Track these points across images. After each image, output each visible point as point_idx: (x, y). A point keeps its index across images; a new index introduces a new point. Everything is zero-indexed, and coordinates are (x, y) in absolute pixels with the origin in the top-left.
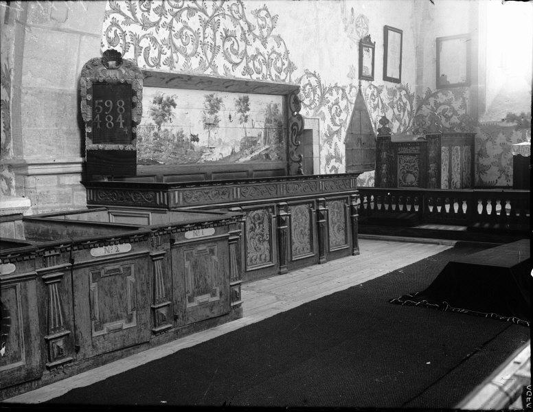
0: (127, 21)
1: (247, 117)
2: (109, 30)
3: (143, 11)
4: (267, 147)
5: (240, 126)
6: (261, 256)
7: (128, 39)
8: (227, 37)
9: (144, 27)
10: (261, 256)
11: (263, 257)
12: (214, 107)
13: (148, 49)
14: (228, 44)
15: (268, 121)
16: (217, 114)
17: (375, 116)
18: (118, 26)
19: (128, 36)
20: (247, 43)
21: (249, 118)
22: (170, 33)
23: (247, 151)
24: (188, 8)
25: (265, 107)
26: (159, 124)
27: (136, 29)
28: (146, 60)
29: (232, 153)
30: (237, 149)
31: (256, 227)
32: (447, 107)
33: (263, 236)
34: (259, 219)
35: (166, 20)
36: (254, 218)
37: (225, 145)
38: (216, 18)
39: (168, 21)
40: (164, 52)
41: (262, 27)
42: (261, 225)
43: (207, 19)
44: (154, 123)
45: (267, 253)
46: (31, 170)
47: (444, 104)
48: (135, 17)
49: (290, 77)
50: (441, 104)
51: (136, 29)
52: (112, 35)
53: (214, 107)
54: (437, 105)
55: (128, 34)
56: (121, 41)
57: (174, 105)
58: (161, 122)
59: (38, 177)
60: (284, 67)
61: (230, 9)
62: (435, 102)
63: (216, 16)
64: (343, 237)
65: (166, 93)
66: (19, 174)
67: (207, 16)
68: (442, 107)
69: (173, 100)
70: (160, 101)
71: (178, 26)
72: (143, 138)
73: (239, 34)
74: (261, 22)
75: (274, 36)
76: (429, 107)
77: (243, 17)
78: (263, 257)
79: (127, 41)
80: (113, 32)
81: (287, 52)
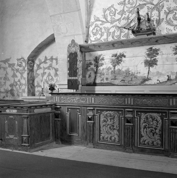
2: (94, 29)
3: (112, 16)
6: (111, 137)
7: (103, 30)
9: (111, 23)
10: (111, 137)
11: (113, 138)
12: (153, 53)
13: (114, 32)
14: (171, 16)
16: (156, 58)
19: (103, 29)
26: (114, 66)
27: (108, 25)
28: (113, 37)
29: (168, 80)
33: (113, 126)
34: (111, 116)
35: (125, 16)
36: (106, 115)
37: (164, 75)
38: (160, 4)
39: (126, 16)
40: (124, 31)
42: (112, 120)
43: (153, 6)
44: (111, 66)
45: (116, 137)
48: (106, 20)
51: (108, 25)
52: (94, 31)
53: (153, 53)
55: (103, 28)
56: (100, 32)
57: (125, 56)
58: (116, 65)
59: (63, 89)
63: (161, 2)
65: (119, 51)
67: (153, 5)
69: (123, 54)
70: (116, 55)
72: (105, 74)
78: (113, 138)
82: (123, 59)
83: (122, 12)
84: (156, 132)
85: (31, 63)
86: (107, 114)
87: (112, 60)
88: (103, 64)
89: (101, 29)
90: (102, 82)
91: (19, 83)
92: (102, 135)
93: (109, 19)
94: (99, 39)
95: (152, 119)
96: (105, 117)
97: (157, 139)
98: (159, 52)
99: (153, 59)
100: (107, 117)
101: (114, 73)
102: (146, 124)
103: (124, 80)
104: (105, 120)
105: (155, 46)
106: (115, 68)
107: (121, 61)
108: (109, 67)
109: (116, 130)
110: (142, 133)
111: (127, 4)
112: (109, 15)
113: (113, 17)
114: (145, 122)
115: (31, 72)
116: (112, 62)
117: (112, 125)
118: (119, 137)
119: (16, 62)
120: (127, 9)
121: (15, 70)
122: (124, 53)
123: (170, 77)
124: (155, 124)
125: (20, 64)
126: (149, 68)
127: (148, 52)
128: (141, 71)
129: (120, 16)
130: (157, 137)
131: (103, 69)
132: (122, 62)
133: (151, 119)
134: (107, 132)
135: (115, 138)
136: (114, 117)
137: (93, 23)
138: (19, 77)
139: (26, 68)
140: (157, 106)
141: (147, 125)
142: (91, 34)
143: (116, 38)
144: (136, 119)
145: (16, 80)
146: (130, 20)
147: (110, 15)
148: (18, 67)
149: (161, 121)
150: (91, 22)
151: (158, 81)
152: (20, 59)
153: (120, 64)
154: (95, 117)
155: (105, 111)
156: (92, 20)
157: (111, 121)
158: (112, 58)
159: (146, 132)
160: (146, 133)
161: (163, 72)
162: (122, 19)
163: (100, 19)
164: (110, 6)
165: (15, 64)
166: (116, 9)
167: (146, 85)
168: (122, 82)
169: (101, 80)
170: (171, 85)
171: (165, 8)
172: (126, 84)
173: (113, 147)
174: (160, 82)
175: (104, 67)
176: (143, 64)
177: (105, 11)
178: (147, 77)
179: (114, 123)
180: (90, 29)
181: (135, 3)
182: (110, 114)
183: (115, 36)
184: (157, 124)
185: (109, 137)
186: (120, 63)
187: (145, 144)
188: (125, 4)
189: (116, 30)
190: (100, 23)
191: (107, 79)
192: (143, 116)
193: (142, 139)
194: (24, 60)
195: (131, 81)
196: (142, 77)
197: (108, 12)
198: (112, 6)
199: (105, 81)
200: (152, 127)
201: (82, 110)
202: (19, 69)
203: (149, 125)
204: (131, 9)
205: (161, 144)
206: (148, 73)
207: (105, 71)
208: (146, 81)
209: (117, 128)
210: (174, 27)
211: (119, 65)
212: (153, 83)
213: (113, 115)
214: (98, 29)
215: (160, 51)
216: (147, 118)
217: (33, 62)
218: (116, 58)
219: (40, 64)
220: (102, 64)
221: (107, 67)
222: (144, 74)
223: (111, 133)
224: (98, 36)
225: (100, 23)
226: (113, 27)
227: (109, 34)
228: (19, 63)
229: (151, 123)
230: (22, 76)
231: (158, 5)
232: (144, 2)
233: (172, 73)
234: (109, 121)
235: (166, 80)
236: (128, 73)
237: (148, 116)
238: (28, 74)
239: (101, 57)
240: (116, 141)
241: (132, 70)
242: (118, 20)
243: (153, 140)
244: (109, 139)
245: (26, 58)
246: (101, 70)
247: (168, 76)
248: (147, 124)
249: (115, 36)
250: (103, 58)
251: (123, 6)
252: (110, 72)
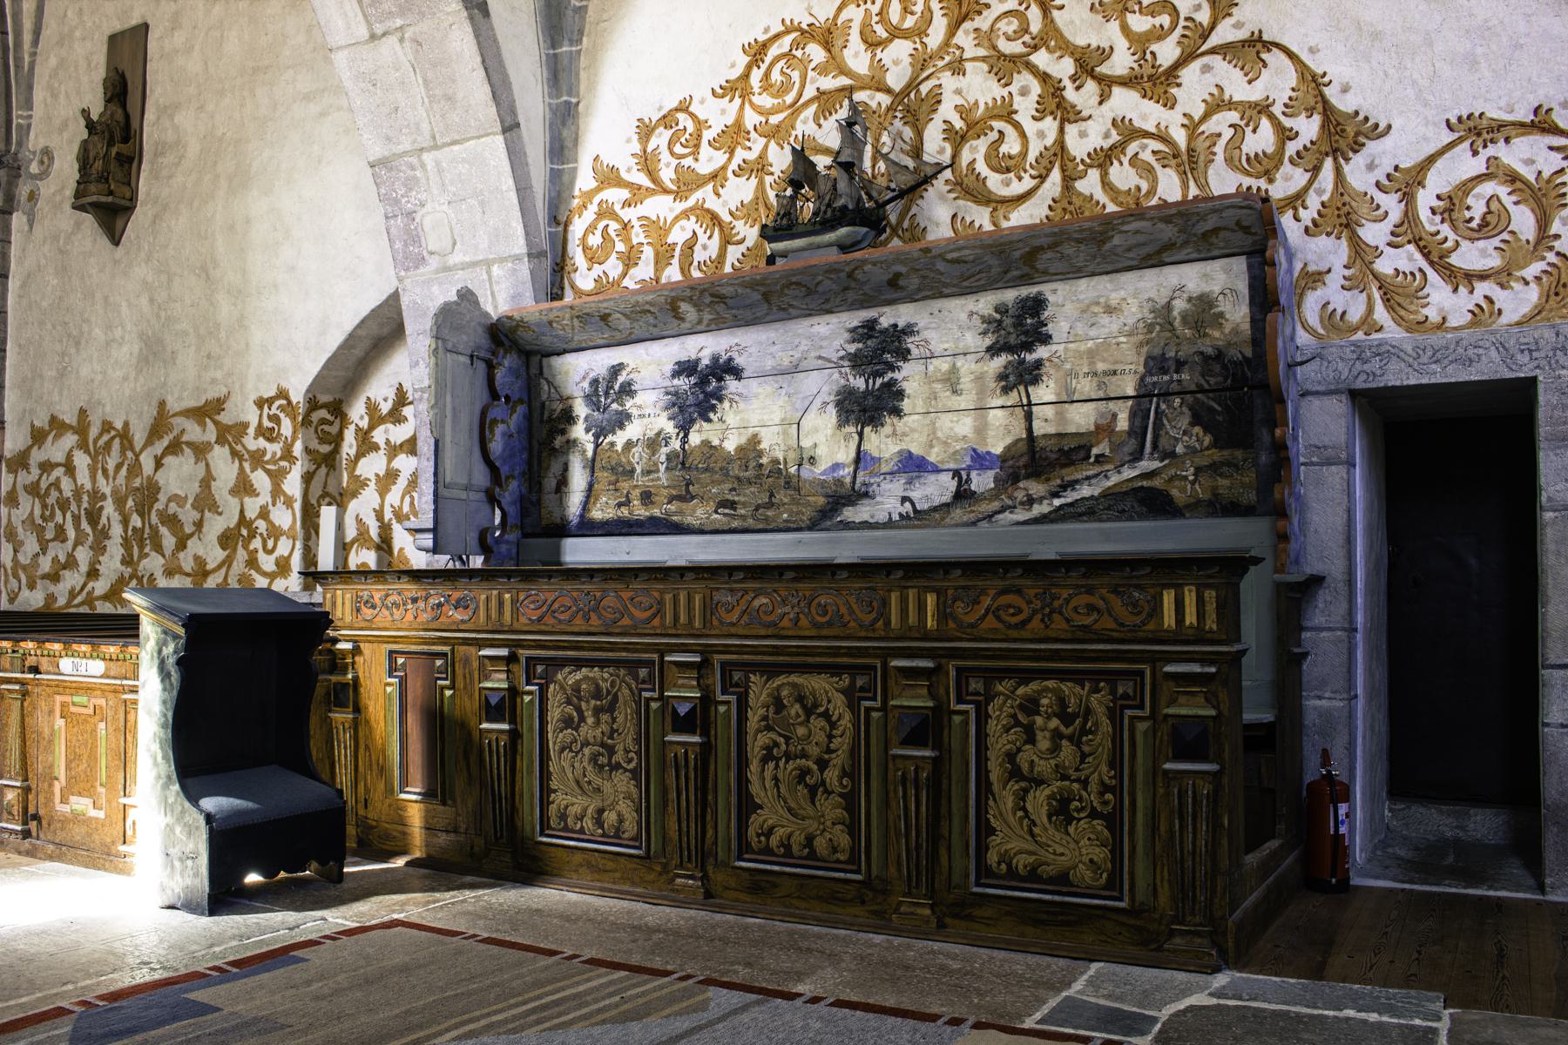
0: (637, 195)
1: (1039, 364)
2: (591, 229)
3: (683, 156)
4: (1147, 465)
5: (999, 402)
6: (601, 811)
7: (638, 236)
8: (972, 126)
9: (679, 195)
10: (601, 811)
11: (610, 817)
13: (690, 246)
14: (975, 153)
15: (1156, 364)
16: (896, 375)
18: (614, 216)
20: (1067, 114)
21: (1047, 368)
22: (761, 183)
23: (1036, 488)
24: (821, 93)
25: (1134, 312)
26: (685, 428)
27: (660, 207)
30: (982, 482)
31: (582, 719)
33: (611, 751)
36: (576, 689)
39: (752, 156)
40: (739, 238)
41: (1140, 43)
42: (605, 717)
43: (885, 100)
44: (670, 428)
45: (625, 807)
48: (654, 181)
49: (1338, 171)
52: (595, 240)
56: (620, 247)
57: (737, 373)
58: (692, 421)
60: (1292, 148)
61: (986, 38)
63: (927, 78)
64: (1100, 854)
65: (704, 347)
67: (888, 91)
69: (731, 359)
72: (639, 470)
73: (1025, 108)
74: (1139, 23)
75: (1223, 50)
77: (1049, 36)
79: (635, 241)
80: (598, 233)
81: (1313, 82)
82: (732, 385)
83: (733, 136)
84: (823, 783)
85: (323, 421)
86: (578, 682)
87: (676, 394)
88: (628, 417)
89: (626, 226)
90: (625, 512)
91: (261, 525)
92: (559, 800)
93: (667, 175)
94: (617, 283)
95: (804, 707)
96: (569, 702)
97: (829, 823)
98: (910, 343)
99: (879, 381)
100: (580, 699)
101: (683, 464)
102: (773, 735)
103: (732, 505)
104: (571, 718)
105: (886, 309)
106: (686, 436)
107: (720, 400)
108: (658, 434)
109: (626, 770)
110: (755, 788)
111: (756, 90)
112: (665, 156)
113: (688, 162)
114: (769, 728)
115: (323, 470)
116: (674, 405)
117: (603, 745)
118: (639, 811)
119: (252, 416)
120: (758, 119)
121: (246, 456)
122: (735, 355)
123: (969, 480)
124: (821, 737)
125: (270, 425)
126: (861, 435)
127: (852, 348)
128: (821, 451)
129: (720, 158)
130: (831, 808)
131: (629, 445)
132: (726, 404)
133: (797, 706)
134: (578, 782)
135: (619, 814)
136: (615, 698)
137: (589, 195)
138: (265, 498)
139: (298, 449)
140: (825, 632)
141: (776, 744)
142: (578, 257)
143: (696, 274)
144: (722, 709)
145: (252, 507)
146: (772, 174)
147: (672, 153)
148: (262, 442)
149: (848, 716)
150: (577, 193)
151: (907, 505)
152: (270, 401)
153: (711, 415)
154: (519, 700)
155: (567, 670)
156: (585, 180)
157: (598, 723)
158: (676, 382)
159: (776, 779)
160: (777, 785)
161: (932, 458)
162: (730, 174)
163: (624, 175)
164: (675, 104)
165: (246, 425)
166: (702, 117)
167: (848, 526)
168: (724, 515)
169: (620, 505)
170: (974, 524)
171: (947, 111)
172: (746, 525)
173: (610, 865)
174: (915, 510)
175: (633, 431)
176: (832, 412)
177: (646, 131)
178: (848, 480)
179: (613, 731)
180: (571, 228)
181: (797, 86)
182: (594, 681)
183: (695, 263)
184: (830, 737)
185: (590, 811)
186: (713, 408)
187: (768, 850)
188: (746, 94)
189: (700, 232)
190: (615, 195)
191: (647, 498)
192: (760, 691)
193: (755, 822)
194: (289, 403)
195: (770, 505)
196: (823, 484)
197: (660, 139)
198: (683, 107)
199: (641, 512)
200: (804, 755)
201: (457, 659)
202: (264, 452)
203: (787, 739)
204: (775, 120)
205: (852, 849)
206: (858, 460)
207: (638, 457)
208: (844, 505)
209: (630, 761)
210: (995, 210)
211: (709, 420)
212: (882, 517)
213: (608, 692)
214: (614, 226)
215: (917, 339)
216: (779, 705)
217: (338, 410)
218: (693, 380)
219: (372, 427)
220: (622, 420)
221: (651, 434)
222: (836, 466)
223: (598, 790)
224: (613, 267)
225: (624, 194)
226: (685, 214)
227: (662, 260)
228: (267, 423)
229: (801, 731)
230: (277, 491)
231: (912, 95)
232: (844, 81)
233: (980, 460)
234: (590, 720)
235: (947, 498)
236: (752, 464)
237: (785, 693)
238: (308, 478)
239: (621, 379)
240: (626, 835)
241: (773, 444)
242: (714, 176)
243: (812, 826)
244: (588, 823)
245: (298, 396)
246: (619, 448)
247: (956, 473)
248: (780, 735)
249: (695, 263)
250: (629, 384)
251: (738, 101)
252: (663, 458)
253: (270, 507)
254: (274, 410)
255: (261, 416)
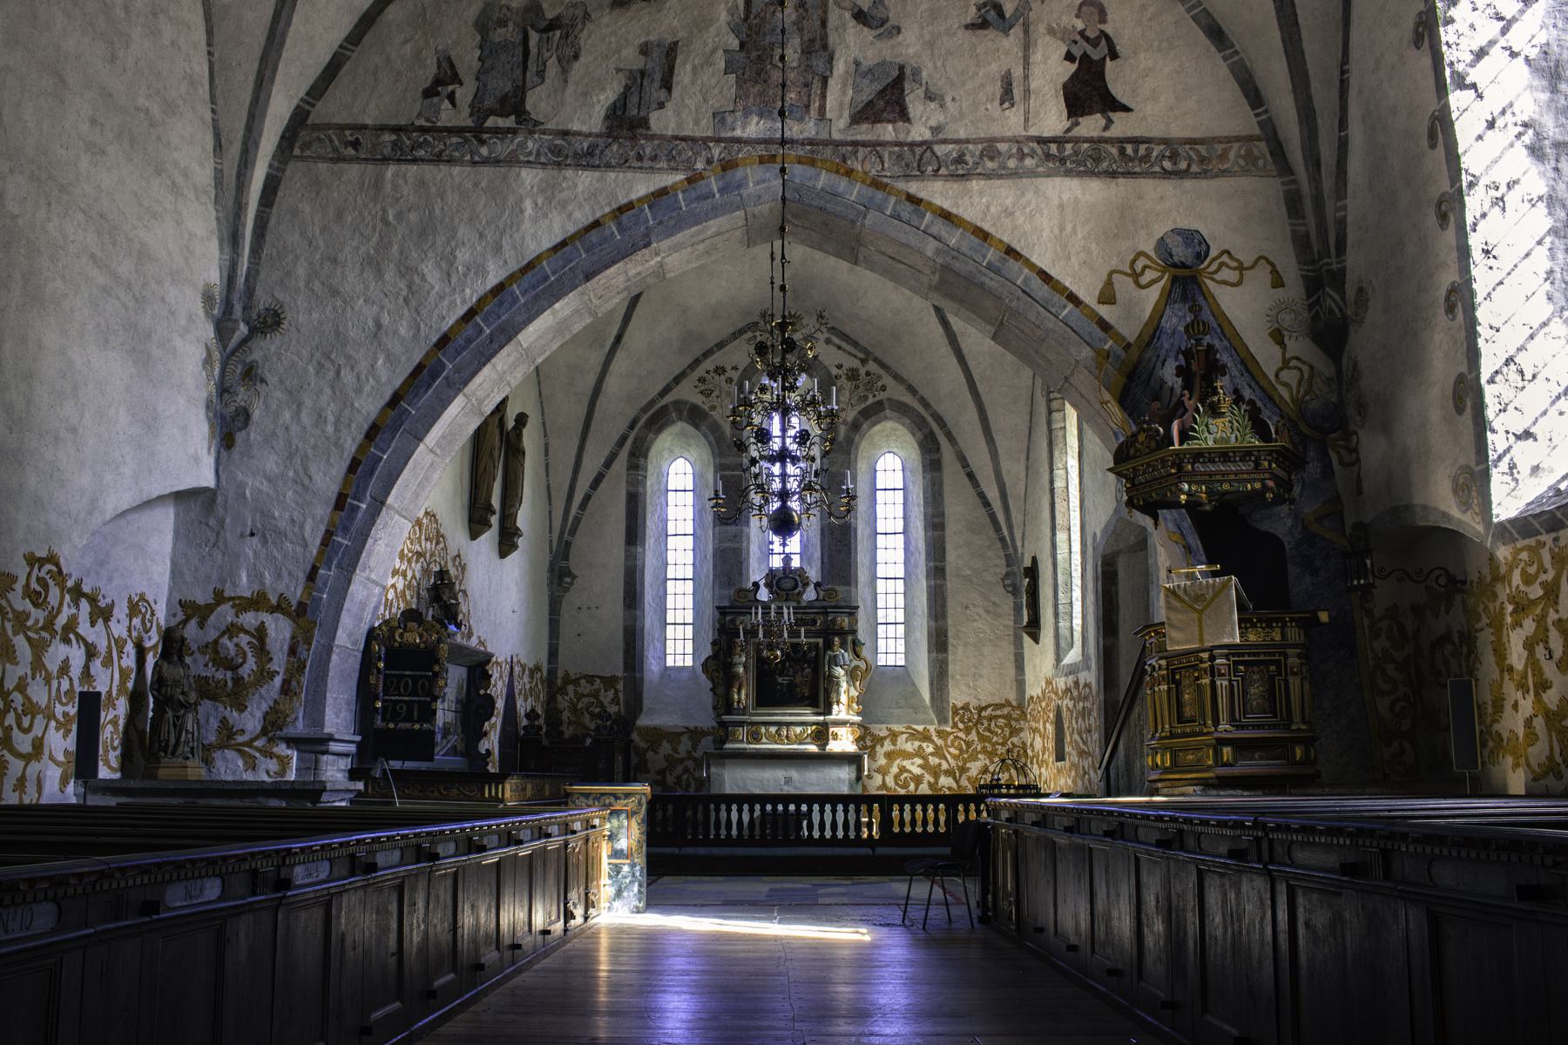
17: (522, 706)
32: (592, 700)
46: (334, 747)
47: (588, 695)
50: (584, 696)
54: (580, 696)
62: (576, 692)
66: (305, 752)
68: (585, 700)
71: (409, 574)
76: (567, 698)
91: (17, 698)
121: (10, 616)
125: (38, 588)
138: (24, 669)
152: (42, 562)
194: (60, 571)
202: (28, 616)
228: (34, 585)
253: (29, 679)
254: (43, 574)
255: (29, 574)
